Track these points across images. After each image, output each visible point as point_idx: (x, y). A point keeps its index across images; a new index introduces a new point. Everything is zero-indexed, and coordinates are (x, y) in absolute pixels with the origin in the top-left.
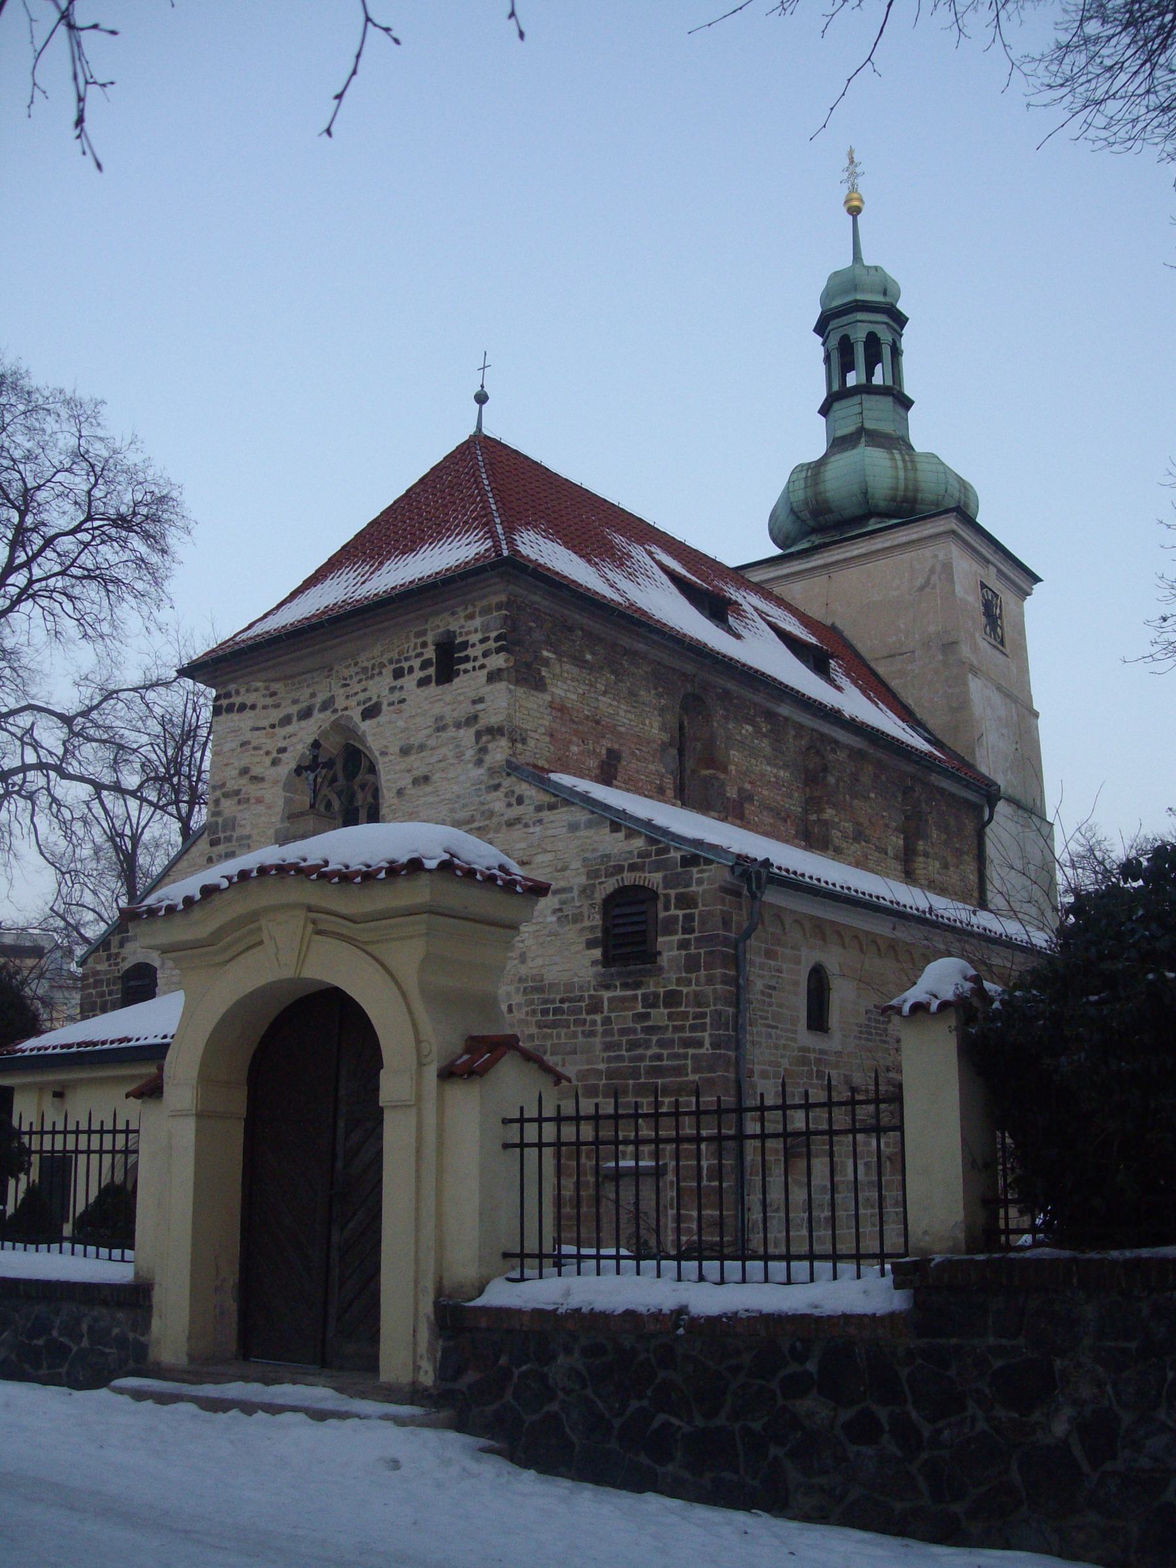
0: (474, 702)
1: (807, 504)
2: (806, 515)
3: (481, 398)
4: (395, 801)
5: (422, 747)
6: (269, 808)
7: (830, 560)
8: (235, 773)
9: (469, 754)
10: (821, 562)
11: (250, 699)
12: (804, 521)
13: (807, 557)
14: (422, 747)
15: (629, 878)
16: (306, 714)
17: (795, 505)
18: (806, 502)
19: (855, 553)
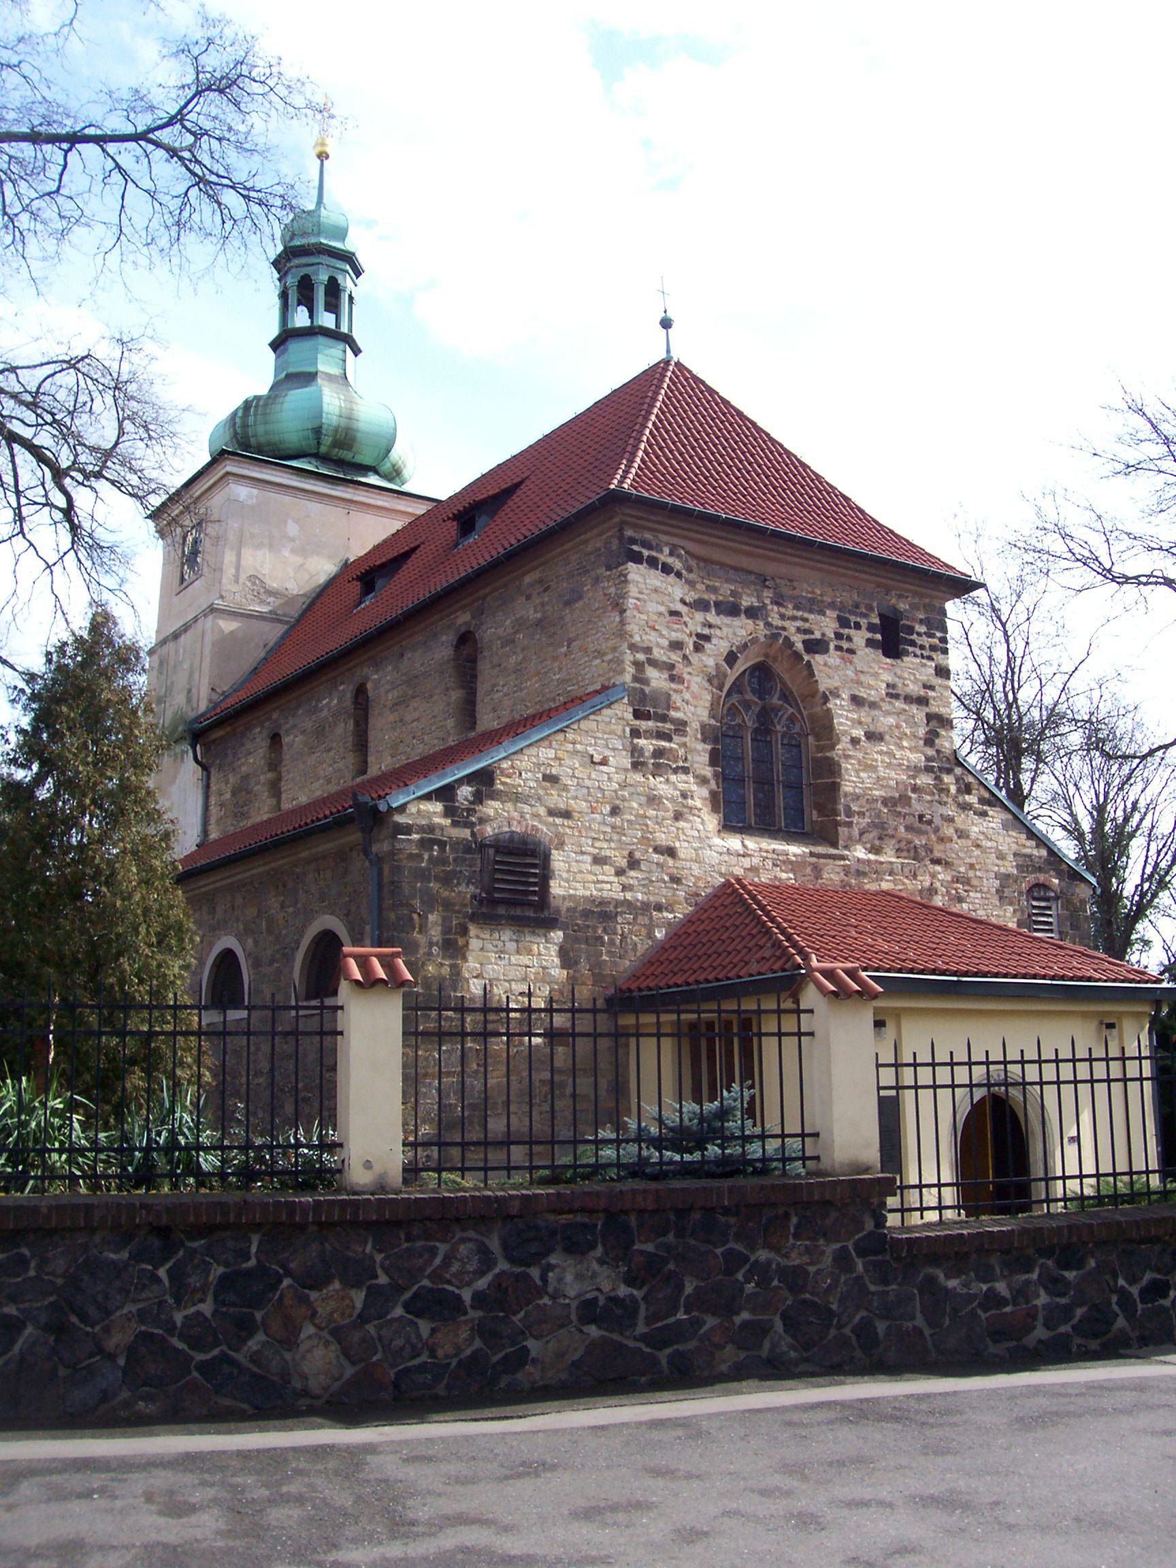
0: (925, 686)
1: (336, 431)
2: (327, 441)
3: (666, 324)
4: (850, 747)
5: (873, 705)
6: (695, 697)
7: (356, 498)
8: (666, 643)
9: (922, 732)
10: (348, 496)
11: (664, 557)
12: (319, 444)
13: (333, 484)
14: (873, 705)
15: (1042, 878)
16: (732, 610)
17: (325, 427)
18: (336, 430)
19: (380, 503)
